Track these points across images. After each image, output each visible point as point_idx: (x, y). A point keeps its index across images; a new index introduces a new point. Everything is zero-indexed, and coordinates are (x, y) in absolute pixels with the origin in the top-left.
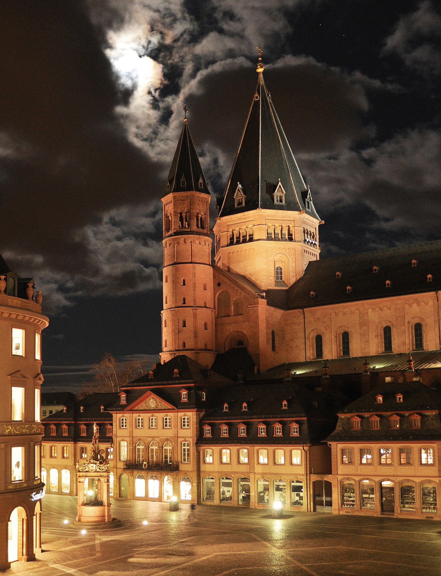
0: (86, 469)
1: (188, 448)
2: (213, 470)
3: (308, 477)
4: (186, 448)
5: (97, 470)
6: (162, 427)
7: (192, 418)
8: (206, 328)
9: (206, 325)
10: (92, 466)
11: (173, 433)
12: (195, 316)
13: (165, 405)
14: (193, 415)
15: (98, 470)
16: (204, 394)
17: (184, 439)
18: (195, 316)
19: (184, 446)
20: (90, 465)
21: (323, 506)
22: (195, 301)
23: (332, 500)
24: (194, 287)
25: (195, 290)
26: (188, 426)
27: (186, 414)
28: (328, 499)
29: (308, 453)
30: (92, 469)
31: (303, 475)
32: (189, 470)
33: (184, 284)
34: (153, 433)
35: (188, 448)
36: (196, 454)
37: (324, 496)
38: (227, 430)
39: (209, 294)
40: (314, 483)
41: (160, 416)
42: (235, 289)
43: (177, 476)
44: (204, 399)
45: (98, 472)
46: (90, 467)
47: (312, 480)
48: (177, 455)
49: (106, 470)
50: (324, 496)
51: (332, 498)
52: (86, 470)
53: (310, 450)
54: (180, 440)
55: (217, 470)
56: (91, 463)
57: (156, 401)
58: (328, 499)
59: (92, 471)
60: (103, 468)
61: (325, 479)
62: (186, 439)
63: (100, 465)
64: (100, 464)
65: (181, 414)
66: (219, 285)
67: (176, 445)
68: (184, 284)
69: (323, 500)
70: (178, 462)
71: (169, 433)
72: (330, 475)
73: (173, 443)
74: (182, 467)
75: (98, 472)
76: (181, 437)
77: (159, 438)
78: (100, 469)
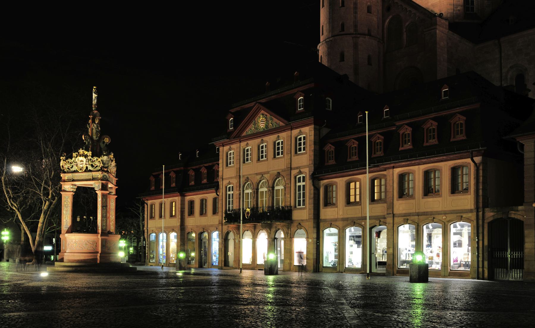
0: (73, 168)
1: (304, 183)
2: (336, 217)
3: (481, 214)
4: (302, 184)
5: (89, 169)
6: (273, 157)
7: (310, 136)
8: (369, 63)
9: (369, 58)
10: (82, 161)
11: (285, 162)
12: (356, 46)
13: (276, 122)
14: (310, 131)
15: (90, 168)
16: (329, 101)
17: (298, 171)
18: (356, 46)
19: (299, 181)
20: (78, 159)
21: (507, 269)
22: (356, 26)
23: (523, 256)
24: (355, 8)
25: (356, 13)
26: (304, 150)
27: (302, 131)
28: (516, 255)
29: (481, 167)
30: (81, 166)
31: (471, 211)
32: (303, 219)
33: (343, 5)
34: (262, 167)
35: (304, 183)
36: (312, 192)
37: (509, 251)
38: (357, 149)
39: (375, 19)
40: (490, 224)
41: (270, 139)
42: (408, 10)
43: (288, 228)
44: (329, 108)
45: (90, 171)
46: (79, 163)
47: (488, 218)
48: (289, 196)
49: (100, 167)
50: (509, 251)
51: (523, 253)
52: (73, 169)
53: (483, 162)
54: (294, 172)
55: (341, 217)
56: (80, 156)
57: (266, 118)
58: (516, 255)
59: (81, 170)
60: (97, 163)
61: (513, 215)
62: (302, 170)
63: (92, 159)
64: (92, 156)
65: (295, 132)
66: (389, 9)
67: (288, 182)
68: (343, 5)
69: (507, 258)
70: (291, 207)
71: (280, 164)
72: (520, 208)
73: (285, 178)
74: (297, 215)
75: (90, 171)
76: (295, 168)
77: (269, 173)
78: (92, 166)
